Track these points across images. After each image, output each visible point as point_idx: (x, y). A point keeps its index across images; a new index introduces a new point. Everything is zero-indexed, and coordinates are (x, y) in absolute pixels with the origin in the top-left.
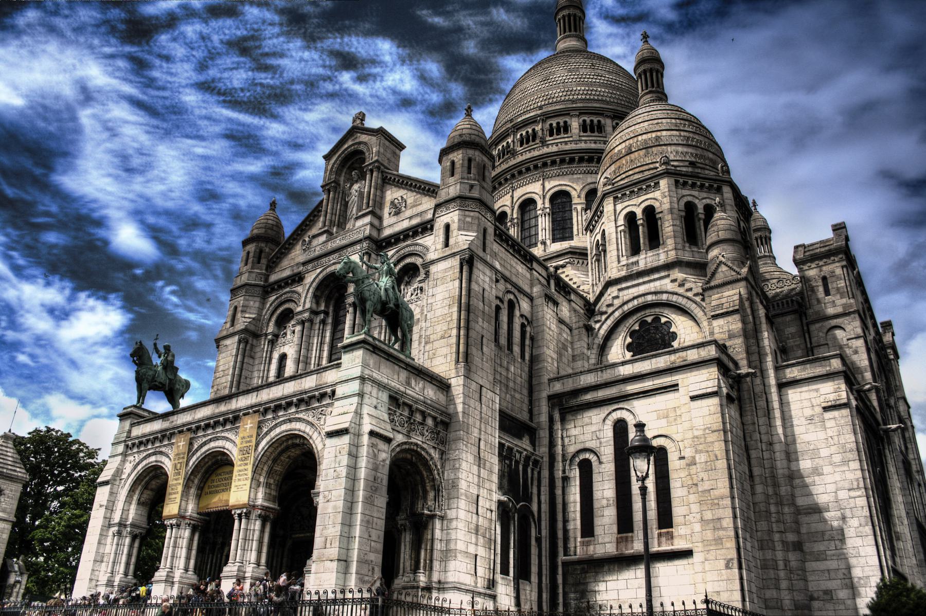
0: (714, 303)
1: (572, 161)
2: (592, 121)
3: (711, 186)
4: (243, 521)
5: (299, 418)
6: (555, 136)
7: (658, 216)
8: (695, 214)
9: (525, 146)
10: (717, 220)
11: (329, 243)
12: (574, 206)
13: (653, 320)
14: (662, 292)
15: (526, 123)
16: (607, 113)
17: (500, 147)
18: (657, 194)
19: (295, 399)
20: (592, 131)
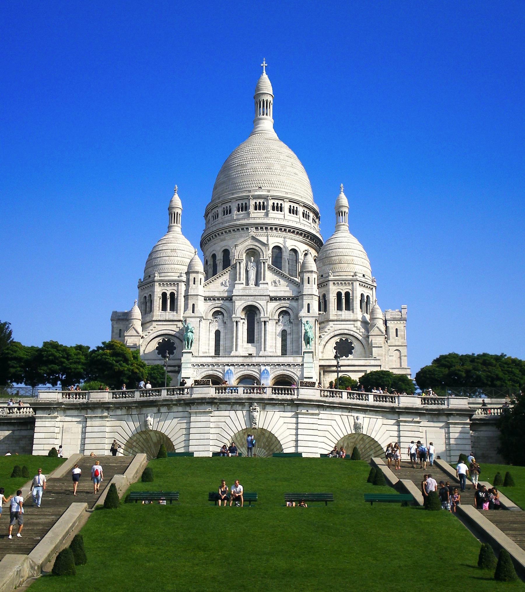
0: (373, 342)
1: (285, 230)
2: (294, 207)
3: (370, 287)
6: (276, 211)
7: (351, 297)
8: (363, 298)
9: (258, 211)
10: (376, 309)
11: (247, 290)
12: (284, 257)
14: (351, 331)
15: (259, 197)
16: (301, 204)
17: (240, 202)
18: (350, 288)
19: (286, 364)
20: (294, 214)
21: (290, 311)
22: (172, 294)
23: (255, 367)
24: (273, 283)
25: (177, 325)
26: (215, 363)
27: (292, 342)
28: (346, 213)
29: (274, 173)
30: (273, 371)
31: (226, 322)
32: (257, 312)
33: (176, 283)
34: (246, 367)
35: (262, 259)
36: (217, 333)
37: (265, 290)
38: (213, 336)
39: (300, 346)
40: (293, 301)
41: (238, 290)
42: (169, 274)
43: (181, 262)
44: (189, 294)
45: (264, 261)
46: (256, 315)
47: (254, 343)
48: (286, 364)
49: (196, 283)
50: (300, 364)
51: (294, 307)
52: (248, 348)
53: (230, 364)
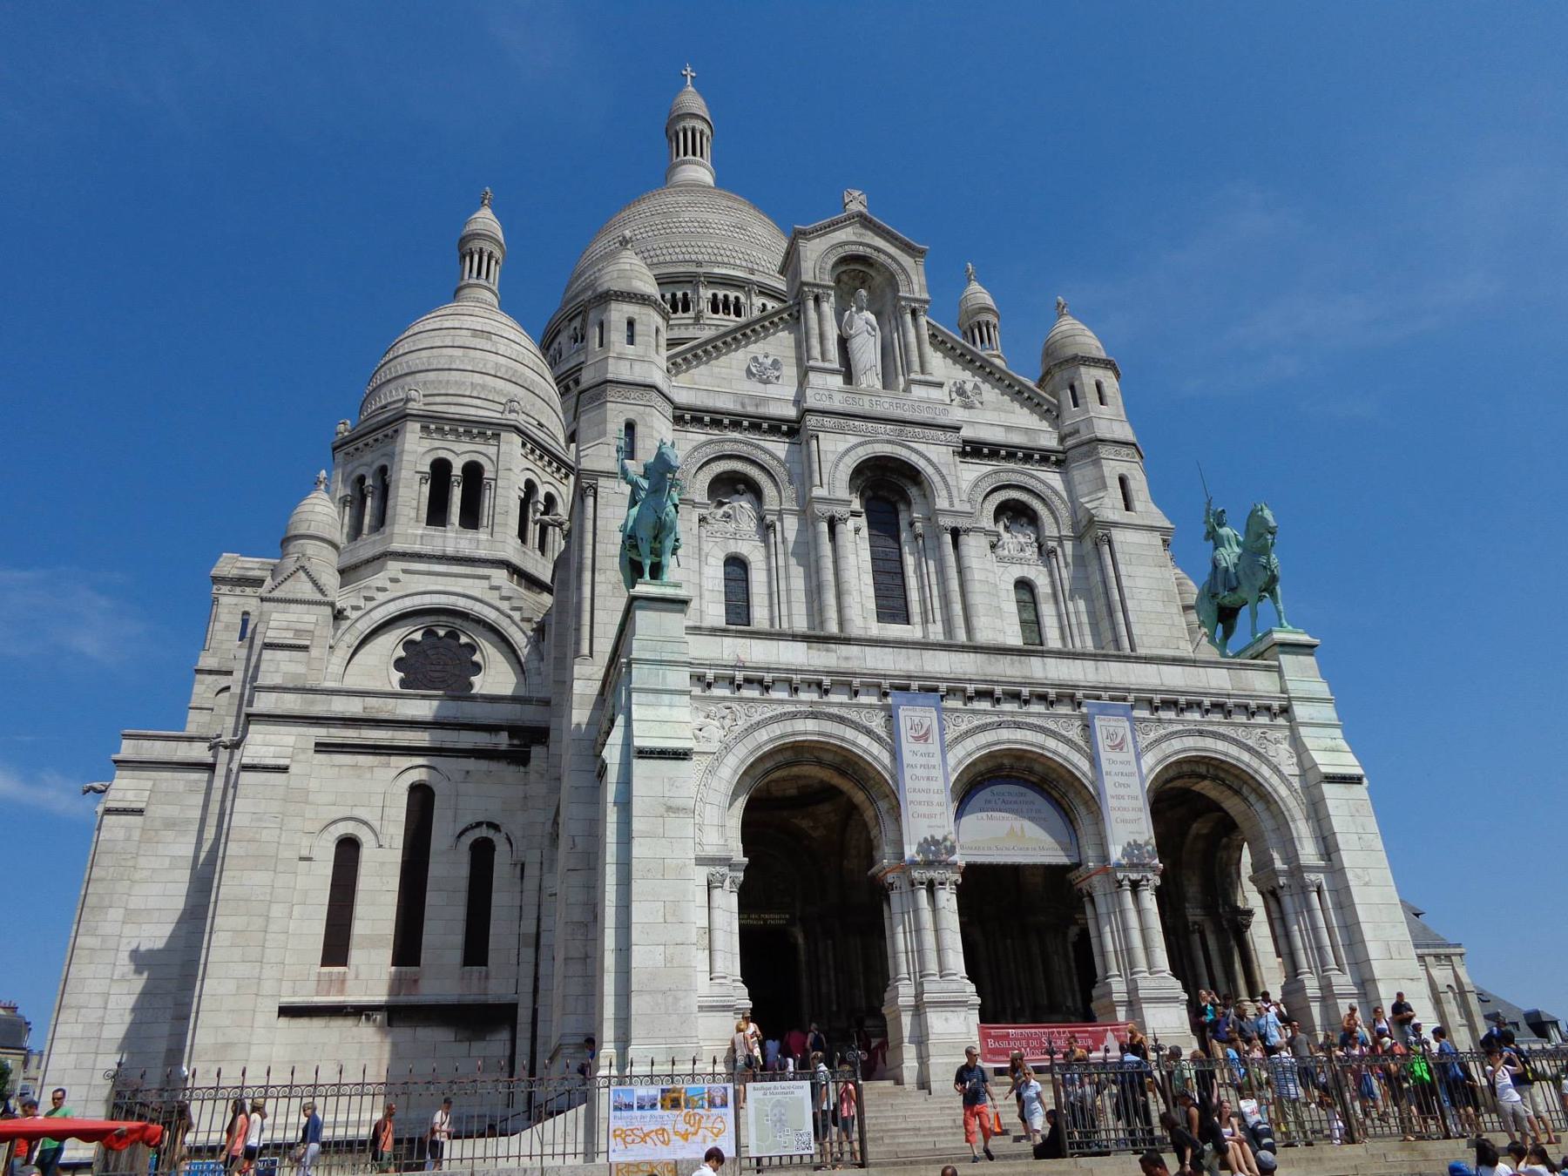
5: (1224, 735)
11: (866, 399)
19: (1207, 702)
21: (1036, 505)
22: (473, 472)
24: (954, 395)
25: (487, 578)
26: (828, 673)
31: (778, 525)
32: (913, 492)
33: (489, 433)
36: (736, 566)
37: (941, 407)
41: (827, 393)
43: (510, 373)
44: (610, 376)
46: (902, 507)
48: (1207, 702)
49: (637, 339)
50: (1276, 705)
51: (1056, 493)
53: (915, 685)
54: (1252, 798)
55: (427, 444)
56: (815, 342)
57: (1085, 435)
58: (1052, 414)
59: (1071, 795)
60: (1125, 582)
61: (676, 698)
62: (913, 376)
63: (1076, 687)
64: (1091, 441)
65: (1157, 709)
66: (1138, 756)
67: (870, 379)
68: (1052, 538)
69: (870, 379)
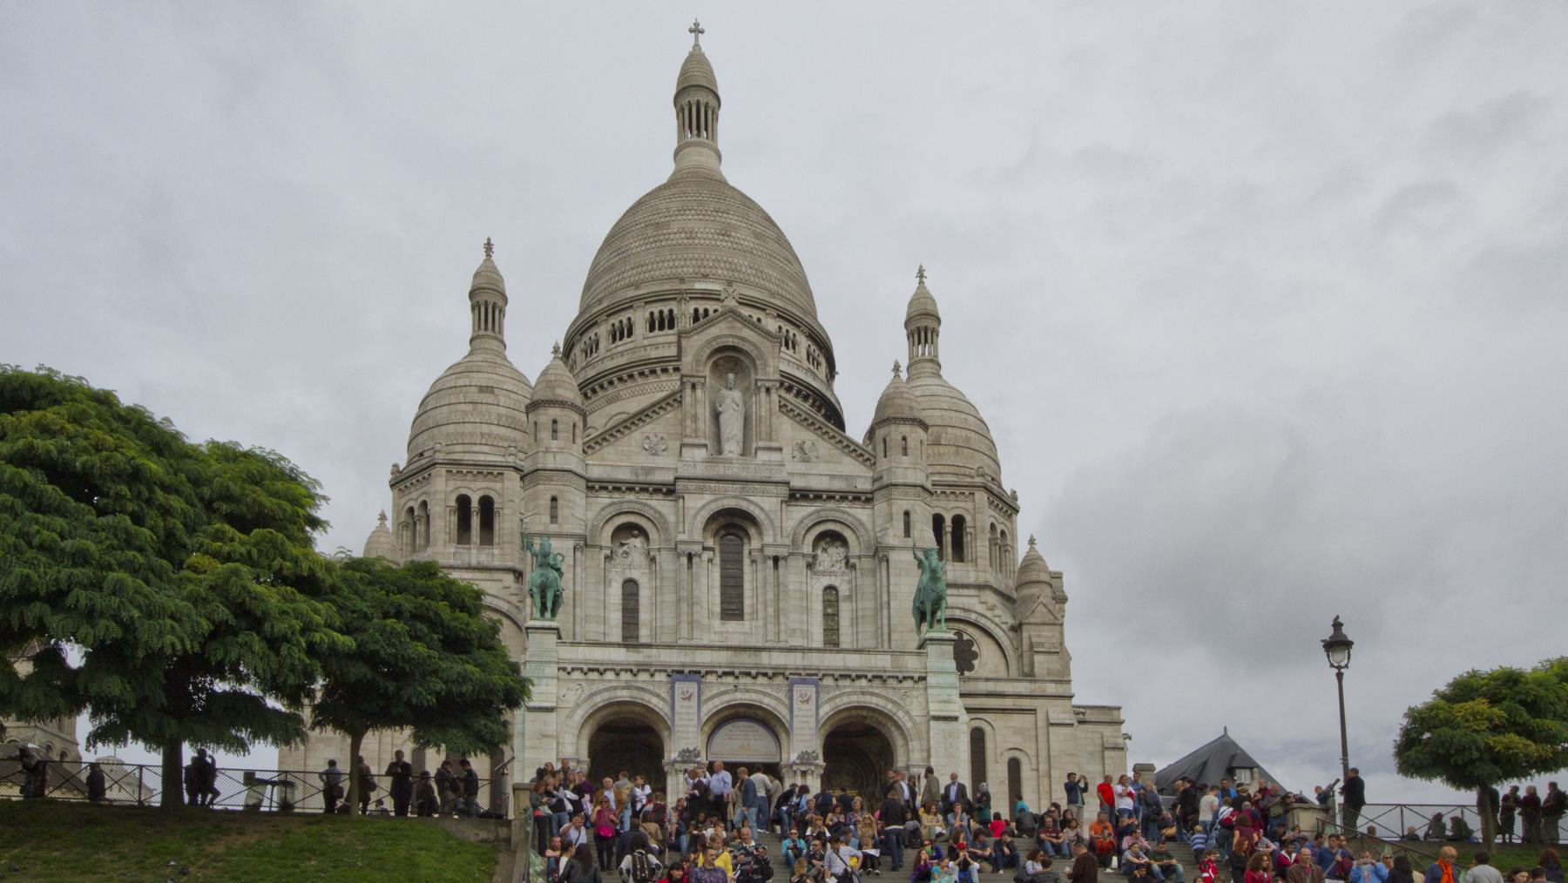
2: (787, 331)
4: (809, 778)
13: (968, 640)
17: (656, 309)
19: (870, 676)
21: (847, 533)
23: (770, 682)
24: (796, 453)
26: (636, 665)
27: (855, 621)
28: (935, 337)
29: (740, 247)
30: (828, 697)
32: (752, 531)
34: (743, 680)
35: (764, 378)
36: (630, 587)
38: (615, 593)
39: (886, 630)
40: (858, 504)
42: (476, 448)
45: (767, 384)
46: (746, 541)
47: (742, 619)
48: (870, 676)
50: (916, 676)
52: (727, 632)
53: (686, 670)
54: (893, 729)
55: (452, 484)
56: (688, 422)
57: (886, 481)
58: (868, 459)
59: (778, 727)
60: (892, 589)
61: (550, 681)
62: (761, 444)
63: (786, 669)
64: (888, 486)
65: (837, 680)
66: (818, 708)
67: (732, 448)
68: (853, 557)
69: (732, 448)
